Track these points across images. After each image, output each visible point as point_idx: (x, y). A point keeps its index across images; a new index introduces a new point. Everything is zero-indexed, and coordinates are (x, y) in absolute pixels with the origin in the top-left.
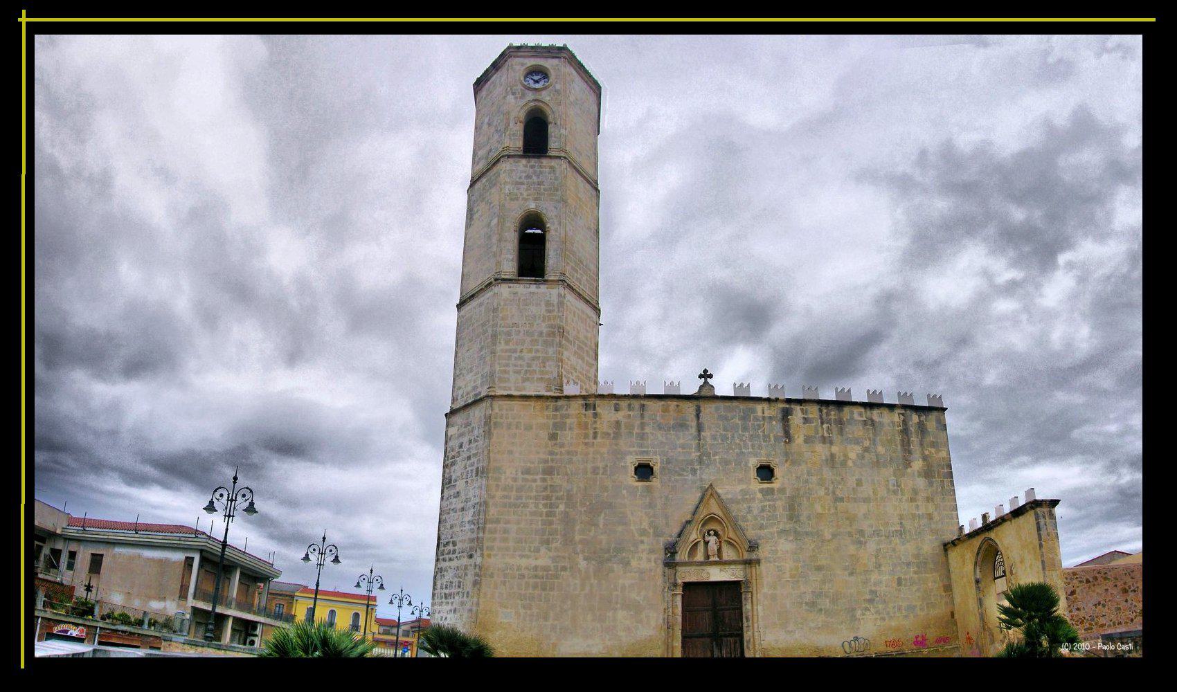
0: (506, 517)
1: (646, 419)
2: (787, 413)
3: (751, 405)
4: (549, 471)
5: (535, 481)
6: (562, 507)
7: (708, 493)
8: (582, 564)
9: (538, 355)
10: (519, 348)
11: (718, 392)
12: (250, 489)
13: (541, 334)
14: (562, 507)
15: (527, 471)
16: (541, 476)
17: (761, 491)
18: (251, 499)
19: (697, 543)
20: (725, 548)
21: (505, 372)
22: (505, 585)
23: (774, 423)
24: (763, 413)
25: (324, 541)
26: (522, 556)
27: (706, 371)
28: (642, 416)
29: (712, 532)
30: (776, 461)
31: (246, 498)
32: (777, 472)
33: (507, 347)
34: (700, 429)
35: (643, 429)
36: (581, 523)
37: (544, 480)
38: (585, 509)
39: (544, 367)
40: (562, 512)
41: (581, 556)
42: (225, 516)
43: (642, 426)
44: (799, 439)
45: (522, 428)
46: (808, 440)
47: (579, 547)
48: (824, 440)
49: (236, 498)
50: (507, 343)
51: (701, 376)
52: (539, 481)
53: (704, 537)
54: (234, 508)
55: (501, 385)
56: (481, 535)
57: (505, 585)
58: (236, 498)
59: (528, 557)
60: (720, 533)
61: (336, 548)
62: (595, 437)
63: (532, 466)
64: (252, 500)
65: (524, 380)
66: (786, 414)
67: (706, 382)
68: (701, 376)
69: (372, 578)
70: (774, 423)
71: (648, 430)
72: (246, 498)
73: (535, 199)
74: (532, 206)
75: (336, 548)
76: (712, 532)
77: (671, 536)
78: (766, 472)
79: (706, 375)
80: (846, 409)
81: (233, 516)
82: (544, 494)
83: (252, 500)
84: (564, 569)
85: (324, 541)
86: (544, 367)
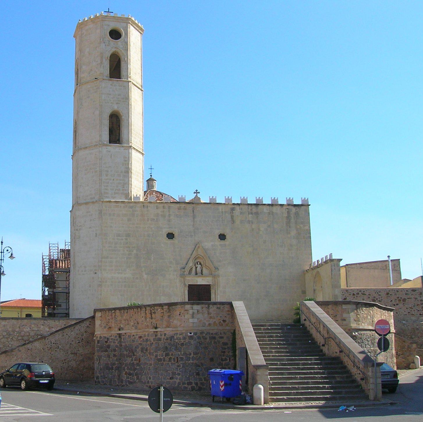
0: (111, 256)
1: (171, 213)
2: (233, 209)
3: (216, 206)
4: (128, 235)
5: (122, 239)
6: (135, 252)
7: (197, 246)
8: (145, 276)
9: (121, 182)
10: (112, 178)
11: (202, 201)
12: (10, 248)
13: (122, 172)
14: (135, 252)
15: (119, 235)
16: (125, 237)
17: (221, 245)
18: (11, 252)
19: (193, 267)
20: (204, 269)
21: (106, 189)
22: (112, 286)
23: (227, 214)
24: (222, 210)
25: (2, 244)
26: (119, 273)
27: (197, 190)
28: (169, 211)
29: (199, 263)
30: (227, 232)
31: (9, 251)
32: (227, 237)
33: (107, 178)
34: (194, 217)
35: (169, 217)
36: (143, 258)
37: (126, 239)
38: (145, 252)
39: (124, 187)
40: (135, 253)
41: (144, 273)
42: (3, 260)
43: (169, 215)
44: (238, 222)
45: (116, 216)
46: (242, 222)
47: (143, 269)
48: (249, 222)
49: (4, 251)
50: (107, 175)
51: (195, 193)
52: (124, 240)
53: (195, 265)
54: (3, 256)
55: (105, 195)
56: (100, 264)
57: (112, 286)
58: (4, 251)
59: (122, 273)
60: (202, 263)
61: (11, 248)
62: (148, 221)
63: (121, 233)
64: (12, 253)
65: (115, 193)
66: (233, 209)
67: (196, 195)
68: (195, 193)
69: (3, 249)
70: (227, 214)
71: (172, 217)
72: (9, 251)
73: (117, 103)
74: (115, 107)
75: (11, 248)
76: (199, 263)
77: (183, 264)
78: (222, 237)
79: (197, 192)
80: (260, 207)
81: (3, 260)
82: (127, 245)
83: (12, 253)
84: (137, 278)
85: (2, 244)
86: (124, 187)
